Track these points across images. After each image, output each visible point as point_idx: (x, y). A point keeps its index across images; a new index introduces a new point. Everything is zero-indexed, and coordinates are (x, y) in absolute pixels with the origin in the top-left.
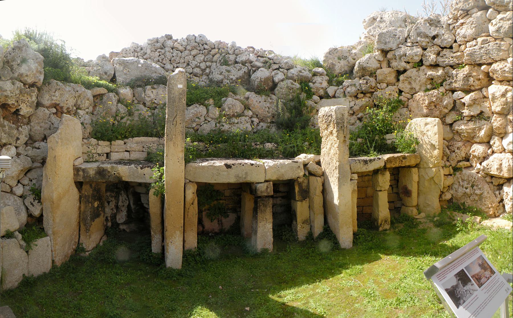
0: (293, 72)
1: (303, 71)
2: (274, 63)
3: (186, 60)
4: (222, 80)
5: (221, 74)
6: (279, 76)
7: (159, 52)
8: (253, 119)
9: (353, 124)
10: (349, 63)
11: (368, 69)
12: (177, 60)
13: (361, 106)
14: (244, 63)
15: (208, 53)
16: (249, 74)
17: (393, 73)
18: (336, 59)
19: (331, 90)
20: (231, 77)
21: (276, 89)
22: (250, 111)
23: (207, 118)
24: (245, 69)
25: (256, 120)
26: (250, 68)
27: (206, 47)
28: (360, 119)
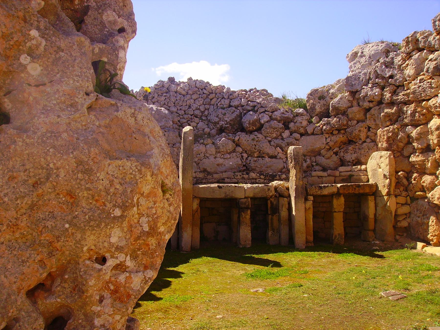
0: (277, 114)
1: (285, 113)
2: (262, 107)
3: (187, 103)
4: (218, 121)
5: (217, 117)
6: (265, 118)
7: (165, 96)
8: (243, 154)
9: (328, 158)
10: (327, 103)
11: (340, 109)
12: (180, 103)
13: (336, 142)
14: (236, 107)
15: (207, 97)
16: (240, 116)
17: (362, 111)
18: (317, 99)
19: (310, 130)
20: (226, 119)
21: (263, 129)
22: (241, 149)
23: (206, 155)
24: (237, 112)
25: (245, 155)
26: (241, 111)
27: (205, 92)
28: (336, 153)
